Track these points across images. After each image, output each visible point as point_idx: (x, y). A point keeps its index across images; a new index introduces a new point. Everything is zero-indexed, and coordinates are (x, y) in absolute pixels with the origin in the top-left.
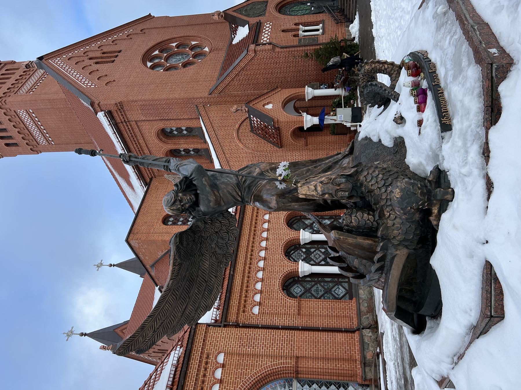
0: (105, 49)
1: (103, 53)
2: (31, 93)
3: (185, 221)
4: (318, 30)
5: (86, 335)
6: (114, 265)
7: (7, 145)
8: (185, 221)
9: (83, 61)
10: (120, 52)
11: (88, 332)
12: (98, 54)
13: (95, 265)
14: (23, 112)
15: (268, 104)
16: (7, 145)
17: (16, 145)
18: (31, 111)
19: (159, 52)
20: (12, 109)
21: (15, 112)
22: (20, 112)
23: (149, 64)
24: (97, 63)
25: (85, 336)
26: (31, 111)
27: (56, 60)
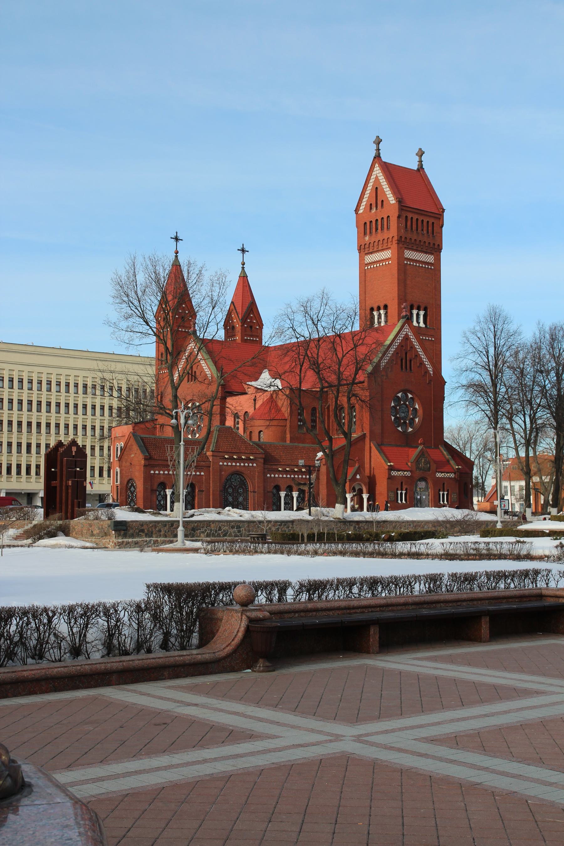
1: (410, 361)
4: (401, 500)
5: (176, 256)
6: (243, 268)
7: (365, 223)
11: (179, 257)
16: (365, 223)
17: (365, 234)
19: (411, 398)
20: (391, 246)
23: (399, 395)
24: (402, 360)
26: (390, 262)
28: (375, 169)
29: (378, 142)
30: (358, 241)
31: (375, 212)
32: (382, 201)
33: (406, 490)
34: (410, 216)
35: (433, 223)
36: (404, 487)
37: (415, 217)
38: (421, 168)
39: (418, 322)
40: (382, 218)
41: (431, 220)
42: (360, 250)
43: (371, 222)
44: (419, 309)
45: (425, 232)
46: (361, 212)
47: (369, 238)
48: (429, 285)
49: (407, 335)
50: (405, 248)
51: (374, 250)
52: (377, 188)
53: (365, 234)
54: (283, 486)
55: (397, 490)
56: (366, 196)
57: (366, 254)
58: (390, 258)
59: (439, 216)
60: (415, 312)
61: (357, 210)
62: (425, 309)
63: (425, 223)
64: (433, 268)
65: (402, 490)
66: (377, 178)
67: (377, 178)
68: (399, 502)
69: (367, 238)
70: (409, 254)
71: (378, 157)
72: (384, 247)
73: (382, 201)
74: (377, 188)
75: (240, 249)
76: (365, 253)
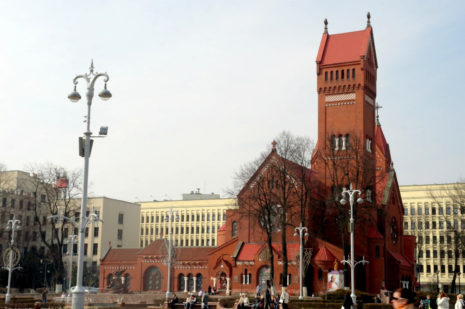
33: (250, 275)
34: (329, 71)
35: (354, 69)
36: (248, 272)
37: (334, 70)
38: (369, 26)
39: (340, 146)
41: (351, 68)
44: (340, 136)
48: (351, 117)
50: (326, 95)
54: (186, 274)
55: (242, 275)
59: (359, 63)
60: (337, 140)
62: (347, 136)
63: (345, 72)
64: (355, 103)
65: (246, 274)
68: (244, 283)
70: (329, 99)
71: (326, 32)
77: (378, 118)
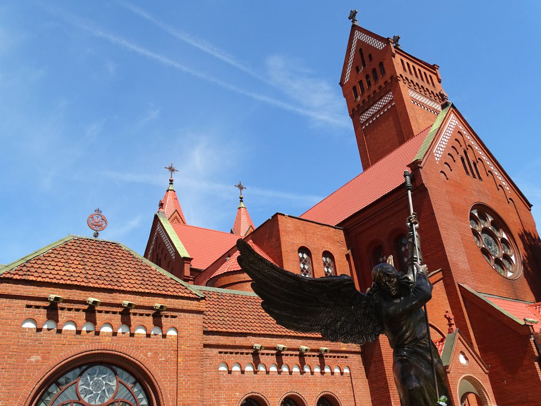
0: (479, 166)
2: (412, 102)
3: (305, 271)
7: (354, 88)
8: (305, 271)
9: (461, 146)
10: (480, 178)
12: (471, 158)
13: (240, 182)
14: (391, 97)
15: (466, 358)
16: (354, 88)
18: (393, 104)
21: (390, 90)
22: (390, 94)
24: (462, 159)
25: (170, 184)
26: (393, 104)
27: (456, 120)
28: (356, 35)
29: (353, 16)
30: (348, 108)
31: (363, 70)
32: (370, 56)
40: (374, 70)
41: (428, 73)
42: (352, 116)
43: (361, 82)
45: (425, 80)
46: (347, 80)
47: (362, 96)
49: (456, 126)
51: (370, 105)
52: (361, 50)
53: (356, 96)
56: (350, 63)
57: (360, 115)
58: (393, 100)
59: (435, 72)
61: (341, 84)
66: (359, 41)
67: (359, 41)
69: (359, 98)
72: (382, 94)
73: (370, 56)
74: (361, 50)
75: (237, 185)
76: (359, 114)
77: (242, 200)
